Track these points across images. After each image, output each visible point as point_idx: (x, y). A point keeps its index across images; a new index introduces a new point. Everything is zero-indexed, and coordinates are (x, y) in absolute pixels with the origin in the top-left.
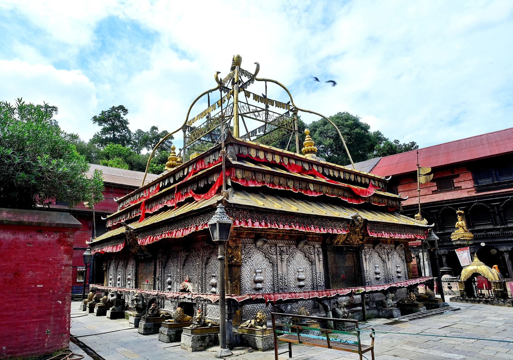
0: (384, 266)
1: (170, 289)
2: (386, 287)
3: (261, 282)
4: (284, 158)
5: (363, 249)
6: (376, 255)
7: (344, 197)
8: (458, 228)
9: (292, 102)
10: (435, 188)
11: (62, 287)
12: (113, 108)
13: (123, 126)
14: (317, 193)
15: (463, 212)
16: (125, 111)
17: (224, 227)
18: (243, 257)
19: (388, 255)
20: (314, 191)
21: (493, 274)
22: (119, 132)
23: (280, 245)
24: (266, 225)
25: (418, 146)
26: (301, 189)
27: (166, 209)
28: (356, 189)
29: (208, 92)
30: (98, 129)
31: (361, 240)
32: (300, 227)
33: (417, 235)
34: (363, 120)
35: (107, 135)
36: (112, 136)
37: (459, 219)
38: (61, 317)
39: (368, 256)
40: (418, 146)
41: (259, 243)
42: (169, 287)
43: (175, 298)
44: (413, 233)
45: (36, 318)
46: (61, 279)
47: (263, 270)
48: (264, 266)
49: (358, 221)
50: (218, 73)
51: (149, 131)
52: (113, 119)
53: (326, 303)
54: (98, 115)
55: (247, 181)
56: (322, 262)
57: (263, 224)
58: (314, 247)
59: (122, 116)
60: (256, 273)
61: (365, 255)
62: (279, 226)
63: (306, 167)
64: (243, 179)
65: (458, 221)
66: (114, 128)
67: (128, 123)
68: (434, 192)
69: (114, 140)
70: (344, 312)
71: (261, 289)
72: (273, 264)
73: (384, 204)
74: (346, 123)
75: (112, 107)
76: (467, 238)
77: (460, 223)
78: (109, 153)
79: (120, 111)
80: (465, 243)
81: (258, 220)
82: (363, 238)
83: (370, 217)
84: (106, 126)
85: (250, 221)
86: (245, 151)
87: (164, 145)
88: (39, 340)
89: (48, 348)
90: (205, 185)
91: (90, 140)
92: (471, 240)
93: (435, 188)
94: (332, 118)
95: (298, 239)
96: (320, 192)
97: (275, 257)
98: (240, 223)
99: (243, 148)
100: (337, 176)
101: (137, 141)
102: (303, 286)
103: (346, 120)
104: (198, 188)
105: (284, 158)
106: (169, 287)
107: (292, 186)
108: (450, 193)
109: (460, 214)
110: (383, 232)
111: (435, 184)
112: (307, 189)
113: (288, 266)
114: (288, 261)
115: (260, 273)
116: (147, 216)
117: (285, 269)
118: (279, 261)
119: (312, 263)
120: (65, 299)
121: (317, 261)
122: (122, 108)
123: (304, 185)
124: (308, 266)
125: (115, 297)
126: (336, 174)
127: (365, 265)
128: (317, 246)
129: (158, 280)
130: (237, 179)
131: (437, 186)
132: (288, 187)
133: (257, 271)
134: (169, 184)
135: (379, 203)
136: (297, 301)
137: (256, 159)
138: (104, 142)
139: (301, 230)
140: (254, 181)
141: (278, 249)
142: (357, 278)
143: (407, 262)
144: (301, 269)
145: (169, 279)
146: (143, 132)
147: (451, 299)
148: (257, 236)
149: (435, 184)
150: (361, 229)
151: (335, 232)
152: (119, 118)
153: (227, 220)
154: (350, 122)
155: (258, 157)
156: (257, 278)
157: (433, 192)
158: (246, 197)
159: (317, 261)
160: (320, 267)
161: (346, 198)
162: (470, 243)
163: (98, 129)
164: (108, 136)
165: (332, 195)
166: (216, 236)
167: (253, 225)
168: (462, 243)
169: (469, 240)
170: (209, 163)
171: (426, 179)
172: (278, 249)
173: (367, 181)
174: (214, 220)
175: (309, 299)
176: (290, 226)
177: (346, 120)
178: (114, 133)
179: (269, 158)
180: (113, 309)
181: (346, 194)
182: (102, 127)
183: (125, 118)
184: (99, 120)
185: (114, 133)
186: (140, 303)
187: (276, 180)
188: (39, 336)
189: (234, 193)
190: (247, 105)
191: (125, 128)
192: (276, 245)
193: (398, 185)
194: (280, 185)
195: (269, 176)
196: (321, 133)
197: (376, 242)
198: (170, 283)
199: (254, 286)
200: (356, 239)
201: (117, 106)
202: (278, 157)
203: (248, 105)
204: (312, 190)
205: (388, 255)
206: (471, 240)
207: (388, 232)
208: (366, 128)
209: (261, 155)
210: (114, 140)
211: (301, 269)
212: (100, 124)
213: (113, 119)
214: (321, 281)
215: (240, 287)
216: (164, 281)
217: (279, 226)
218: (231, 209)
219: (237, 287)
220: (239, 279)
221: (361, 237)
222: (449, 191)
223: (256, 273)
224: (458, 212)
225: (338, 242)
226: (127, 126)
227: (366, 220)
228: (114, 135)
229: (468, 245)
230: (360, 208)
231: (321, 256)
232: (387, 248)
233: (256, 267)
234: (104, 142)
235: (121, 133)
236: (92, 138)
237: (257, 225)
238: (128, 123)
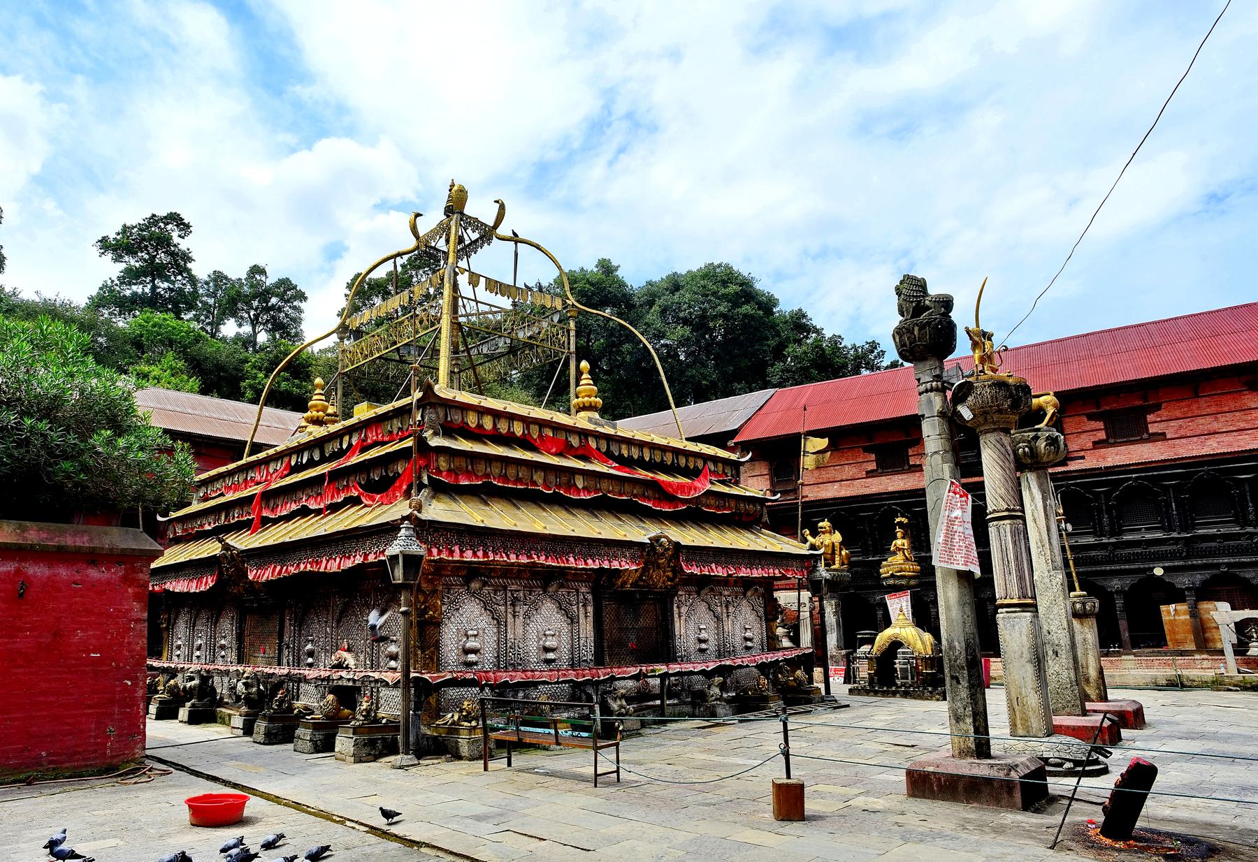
0: (717, 628)
1: (310, 665)
2: (712, 666)
3: (475, 651)
4: (532, 427)
5: (676, 594)
6: (702, 607)
7: (644, 497)
8: (894, 553)
10: (873, 466)
11: (132, 657)
12: (154, 220)
13: (178, 266)
14: (589, 492)
15: (905, 520)
17: (411, 562)
19: (727, 607)
21: (923, 643)
22: (167, 279)
23: (514, 587)
24: (486, 555)
25: (883, 352)
26: (559, 487)
27: (304, 512)
28: (670, 484)
29: (394, 257)
30: (110, 269)
31: (669, 579)
32: (547, 558)
33: (787, 571)
34: (763, 285)
35: (134, 288)
36: (147, 290)
37: (899, 535)
38: (131, 706)
39: (684, 610)
40: (883, 352)
41: (475, 585)
42: (310, 660)
43: (323, 680)
44: (776, 566)
45: (90, 707)
46: (129, 643)
48: (482, 625)
49: (661, 545)
50: (418, 215)
51: (244, 276)
52: (151, 247)
53: (590, 691)
54: (112, 236)
55: (457, 475)
56: (591, 619)
57: (480, 554)
58: (577, 591)
59: (176, 239)
60: (467, 636)
61: (678, 607)
62: (508, 556)
63: (575, 441)
64: (449, 471)
65: (896, 538)
66: (154, 271)
67: (190, 260)
68: (870, 474)
69: (153, 302)
70: (621, 707)
71: (476, 663)
72: (499, 622)
73: (729, 508)
74: (723, 291)
75: (149, 215)
77: (899, 542)
78: (141, 336)
79: (169, 227)
80: (904, 582)
82: (675, 576)
83: (690, 536)
84: (134, 263)
85: (456, 548)
86: (456, 417)
87: (282, 315)
88: (97, 744)
89: (112, 757)
90: (382, 477)
91: (91, 298)
93: (873, 466)
94: (692, 276)
95: (545, 580)
96: (596, 491)
97: (503, 608)
98: (440, 552)
99: (453, 411)
100: (636, 457)
101: (211, 301)
102: (554, 661)
103: (725, 283)
104: (369, 480)
105: (532, 427)
106: (310, 660)
107: (540, 481)
108: (900, 477)
109: (900, 524)
110: (713, 566)
111: (873, 457)
112: (571, 486)
113: (525, 624)
114: (527, 616)
115: (475, 636)
116: (265, 522)
117: (520, 631)
118: (509, 616)
119: (573, 620)
120: (137, 677)
121: (582, 616)
122: (175, 218)
123: (564, 479)
124: (565, 625)
125: (196, 682)
126: (635, 453)
127: (677, 625)
128: (583, 590)
129: (288, 647)
130: (439, 472)
131: (876, 461)
132: (535, 483)
133: (470, 633)
134: (312, 464)
135: (718, 508)
136: (535, 685)
137: (477, 431)
138: (127, 305)
139: (550, 563)
140: (469, 474)
141: (509, 594)
142: (664, 648)
143: (767, 620)
144: (551, 633)
145: (309, 646)
146: (226, 278)
147: (850, 690)
148: (470, 573)
149: (873, 457)
150: (670, 561)
151: (615, 565)
152: (169, 245)
153: (417, 548)
154: (733, 288)
155: (480, 426)
156: (468, 645)
157: (868, 472)
158: (454, 506)
159: (582, 616)
160: (587, 628)
161: (649, 501)
162: (912, 582)
163: (110, 269)
164: (138, 289)
165: (621, 495)
166: (398, 575)
167: (461, 556)
168: (898, 582)
170: (391, 432)
171: (817, 461)
172: (509, 594)
173: (700, 464)
174: (394, 549)
175: (557, 683)
176: (530, 557)
177: (725, 283)
178: (153, 281)
179: (503, 427)
180: (193, 705)
181: (649, 493)
182: (122, 266)
183: (184, 244)
184: (116, 247)
185: (153, 281)
186: (254, 690)
187: (511, 472)
188: (96, 737)
189: (433, 497)
190: (473, 304)
191: (183, 270)
192: (505, 588)
194: (518, 480)
195: (499, 464)
196: (664, 312)
197: (702, 584)
198: (311, 654)
199: (463, 658)
200: (660, 578)
201: (162, 213)
202: (520, 424)
203: (477, 302)
204: (580, 486)
205: (727, 607)
207: (725, 565)
208: (768, 305)
209: (488, 423)
210: (153, 302)
211: (551, 633)
212: (118, 259)
213: (151, 247)
214: (588, 652)
216: (299, 650)
217: (508, 556)
218: (425, 529)
219: (432, 660)
220: (437, 645)
221: (670, 574)
222: (898, 473)
223: (467, 636)
224: (897, 520)
225: (625, 583)
226: (189, 265)
227: (678, 543)
228: (154, 288)
230: (679, 519)
231: (590, 609)
232: (726, 593)
233: (468, 628)
234: (127, 305)
235: (173, 283)
236: (94, 294)
237: (469, 556)
238: (190, 260)
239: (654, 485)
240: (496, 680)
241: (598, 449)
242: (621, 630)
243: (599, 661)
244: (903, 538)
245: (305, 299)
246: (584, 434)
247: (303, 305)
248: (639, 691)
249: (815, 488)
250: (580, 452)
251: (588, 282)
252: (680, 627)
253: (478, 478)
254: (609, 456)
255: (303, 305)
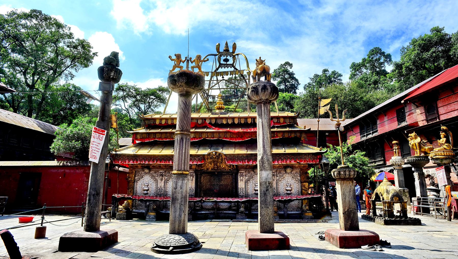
7: (226, 138)
9: (248, 66)
14: (197, 139)
16: (291, 65)
18: (136, 178)
20: (194, 138)
23: (161, 171)
24: (137, 162)
37: (442, 136)
44: (293, 159)
47: (150, 185)
57: (135, 162)
71: (147, 194)
72: (156, 181)
73: (277, 136)
76: (439, 157)
81: (132, 160)
85: (127, 161)
86: (152, 122)
92: (446, 159)
96: (200, 138)
97: (157, 178)
98: (121, 162)
109: (444, 131)
126: (230, 122)
140: (149, 138)
143: (301, 182)
155: (160, 123)
169: (442, 159)
187: (163, 136)
193: (438, 100)
194: (166, 138)
206: (446, 159)
215: (133, 192)
229: (445, 164)
239: (229, 132)
240: (139, 198)
241: (210, 123)
242: (211, 185)
243: (197, 194)
244: (445, 137)
245: (342, 76)
246: (204, 119)
247: (341, 78)
248: (213, 207)
249: (445, 115)
250: (204, 125)
251: (423, 40)
252: (241, 185)
253: (151, 139)
254: (216, 125)
255: (341, 78)
